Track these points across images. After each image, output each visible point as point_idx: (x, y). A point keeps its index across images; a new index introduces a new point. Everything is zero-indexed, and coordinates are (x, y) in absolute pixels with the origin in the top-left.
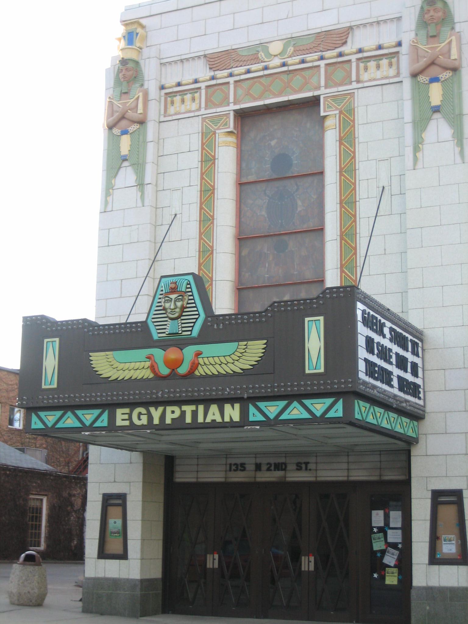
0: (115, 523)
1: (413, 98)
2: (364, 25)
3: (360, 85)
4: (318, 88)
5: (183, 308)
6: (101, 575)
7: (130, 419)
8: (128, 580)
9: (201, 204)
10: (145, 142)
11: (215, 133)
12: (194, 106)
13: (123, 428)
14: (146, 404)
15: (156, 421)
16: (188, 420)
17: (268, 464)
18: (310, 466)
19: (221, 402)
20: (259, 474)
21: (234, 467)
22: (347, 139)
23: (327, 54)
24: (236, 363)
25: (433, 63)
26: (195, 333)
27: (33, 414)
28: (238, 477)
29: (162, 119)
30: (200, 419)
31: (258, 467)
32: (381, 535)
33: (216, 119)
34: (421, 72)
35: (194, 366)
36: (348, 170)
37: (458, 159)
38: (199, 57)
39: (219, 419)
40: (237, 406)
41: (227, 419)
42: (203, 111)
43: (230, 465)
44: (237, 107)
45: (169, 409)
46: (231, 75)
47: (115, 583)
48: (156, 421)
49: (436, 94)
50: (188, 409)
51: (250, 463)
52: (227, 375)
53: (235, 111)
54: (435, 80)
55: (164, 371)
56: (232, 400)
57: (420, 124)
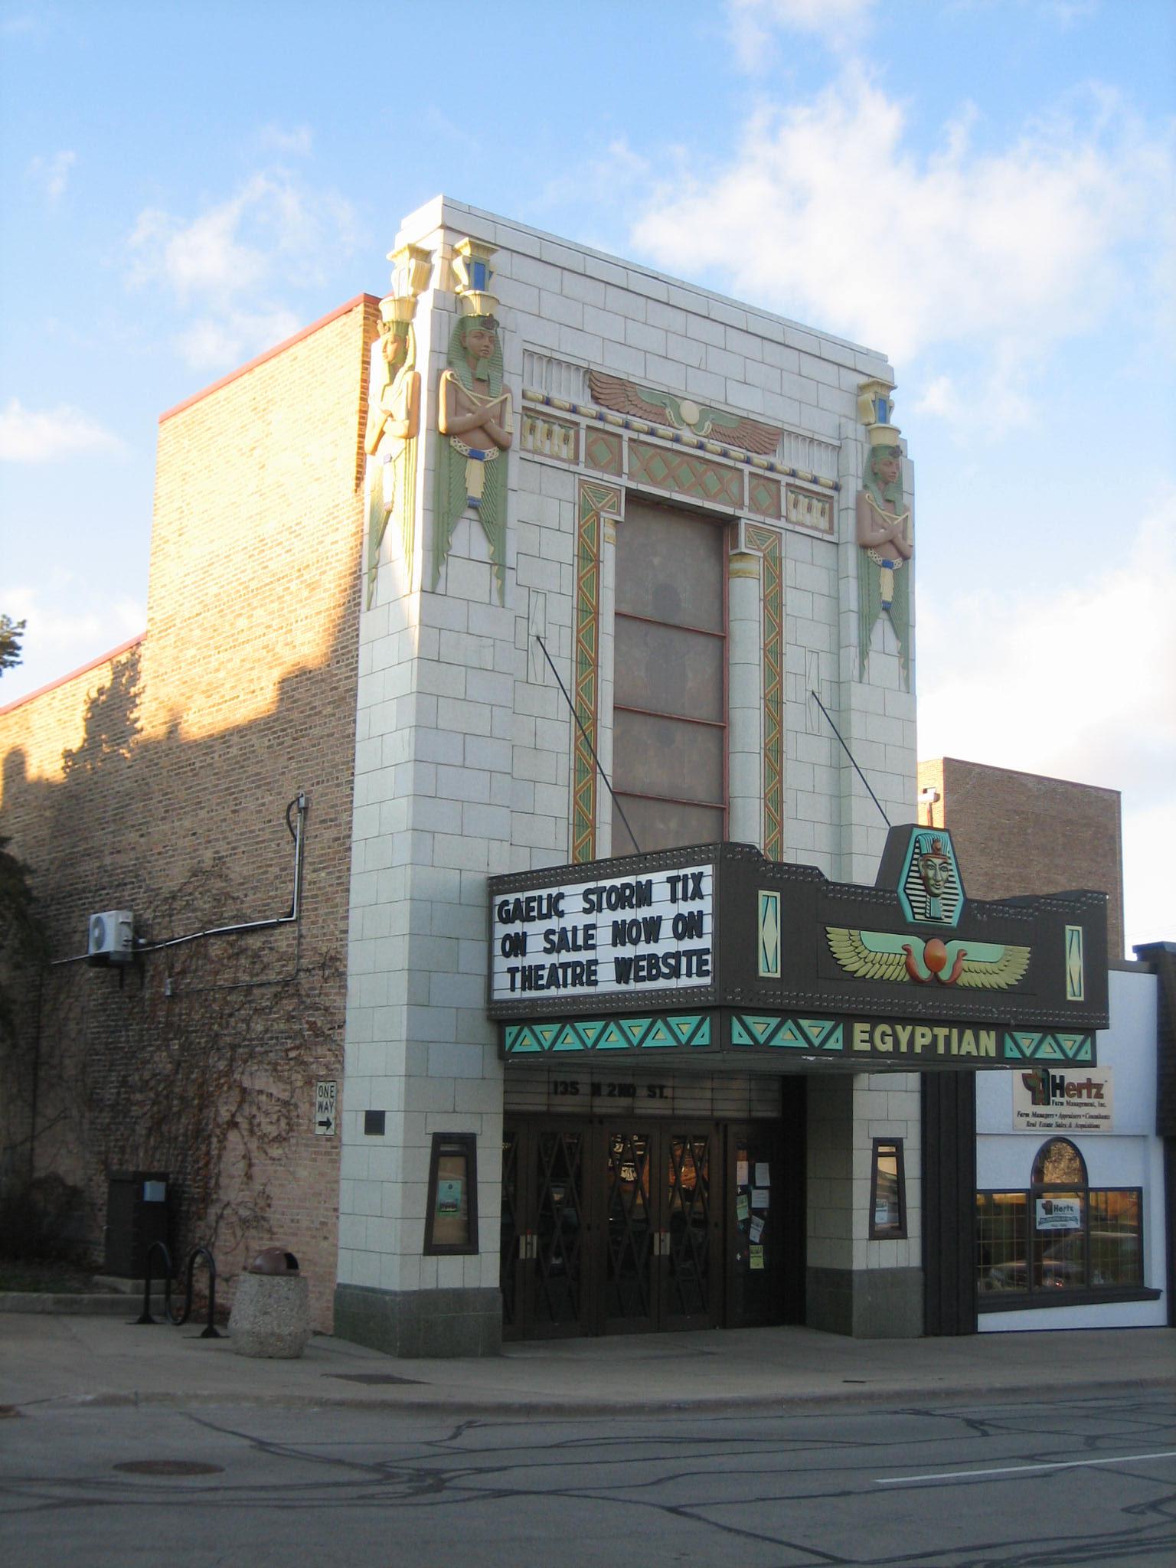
0: (450, 1187)
1: (859, 578)
3: (790, 527)
4: (741, 506)
6: (430, 1285)
7: (871, 1041)
8: (478, 1289)
11: (598, 515)
12: (566, 452)
13: (862, 1054)
14: (892, 1020)
15: (904, 1048)
16: (941, 1050)
17: (610, 1085)
18: (668, 1092)
19: (977, 1026)
20: (597, 1101)
21: (561, 1089)
22: (774, 605)
23: (756, 458)
26: (954, 922)
27: (734, 1019)
28: (568, 1104)
30: (954, 1051)
31: (596, 1090)
32: (744, 1197)
33: (602, 491)
37: (903, 688)
38: (578, 368)
40: (993, 1034)
41: (983, 1054)
43: (556, 1084)
44: (633, 485)
45: (919, 1030)
46: (627, 426)
47: (459, 1297)
48: (904, 1048)
50: (942, 1032)
51: (584, 1079)
53: (629, 491)
55: (924, 973)
56: (988, 1026)
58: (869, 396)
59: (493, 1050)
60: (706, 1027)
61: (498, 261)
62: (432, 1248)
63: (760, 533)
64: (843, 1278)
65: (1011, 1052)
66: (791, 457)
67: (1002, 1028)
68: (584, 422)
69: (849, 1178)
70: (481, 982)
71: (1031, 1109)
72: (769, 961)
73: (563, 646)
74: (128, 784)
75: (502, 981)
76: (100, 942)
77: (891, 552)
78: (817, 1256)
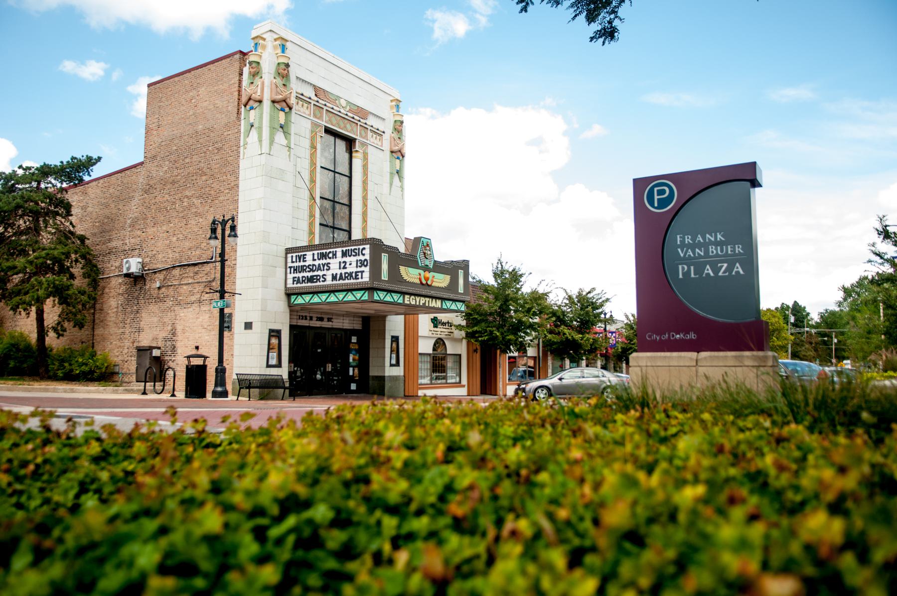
12: (307, 112)
22: (365, 167)
33: (318, 125)
35: (433, 281)
42: (312, 118)
50: (427, 299)
55: (424, 282)
58: (394, 103)
59: (286, 303)
60: (366, 294)
61: (288, 45)
62: (268, 366)
63: (364, 144)
64: (382, 379)
65: (445, 307)
66: (371, 121)
68: (313, 102)
69: (384, 348)
70: (283, 281)
71: (433, 329)
72: (385, 276)
73: (306, 176)
74: (136, 214)
75: (290, 281)
76: (128, 268)
77: (399, 154)
78: (373, 372)
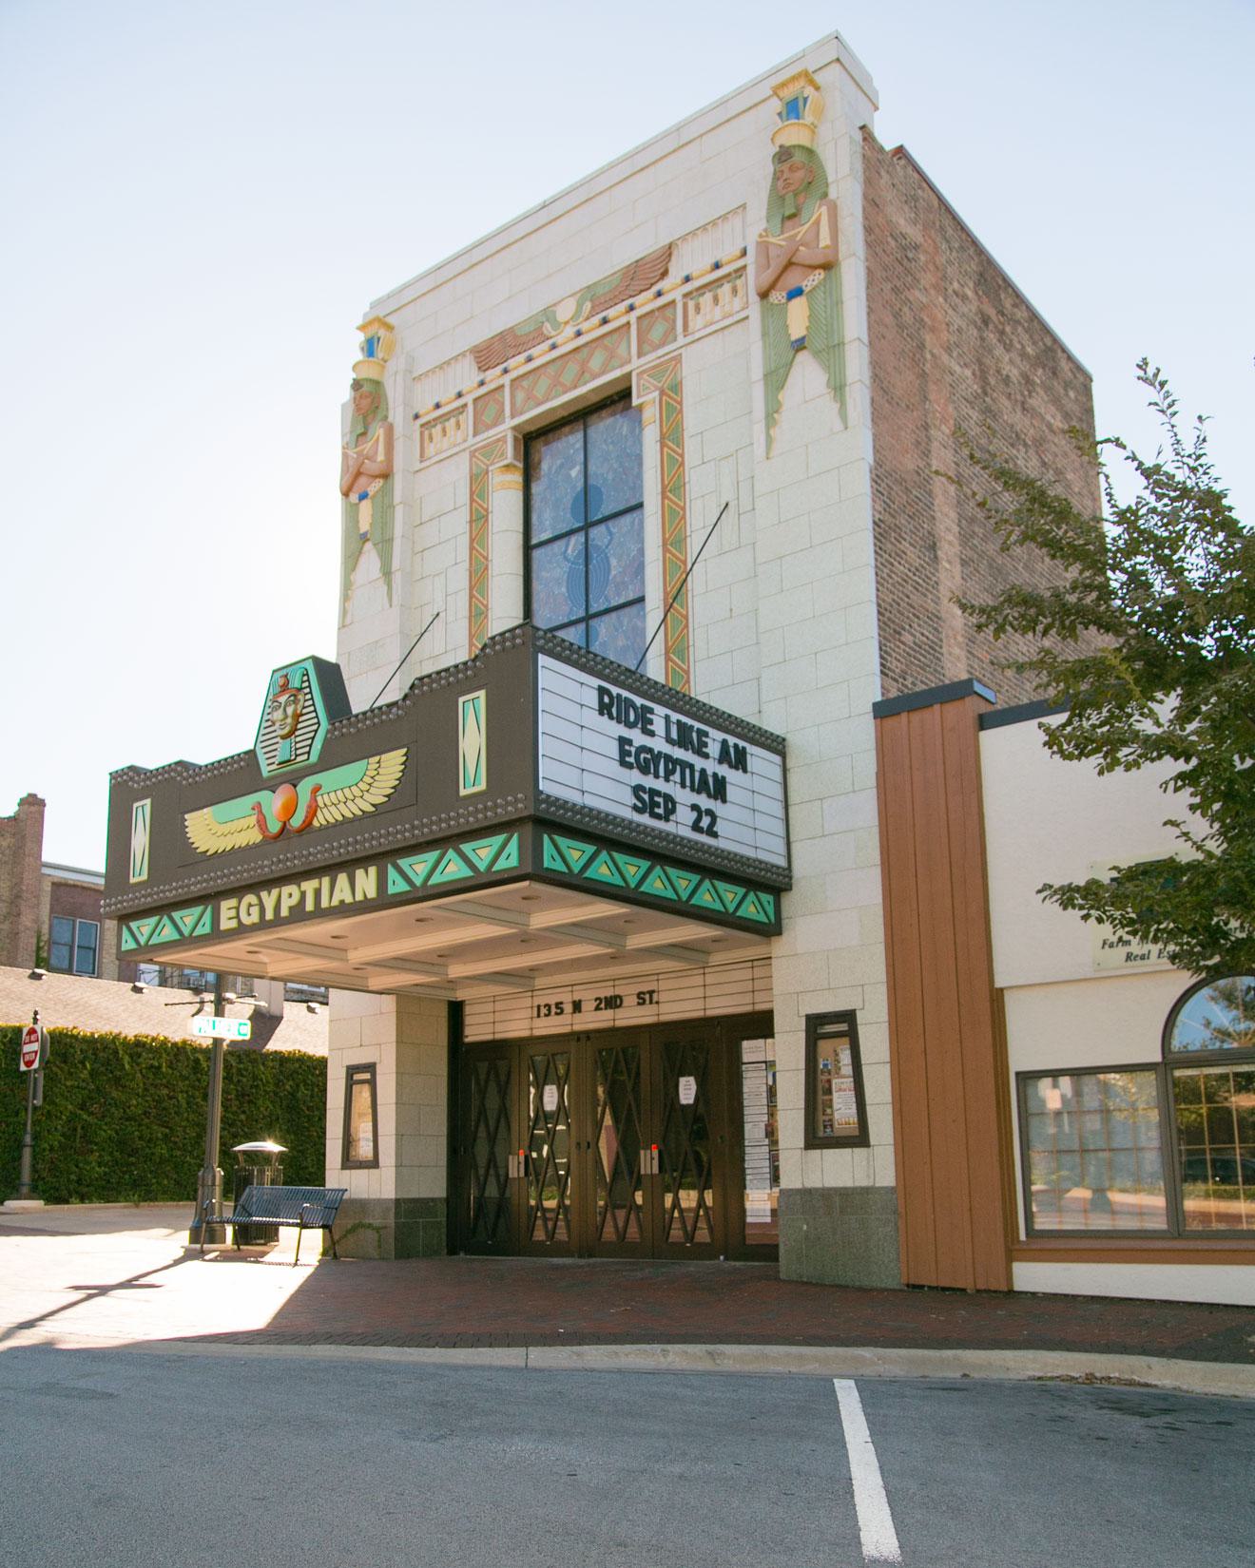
2: (693, 233)
3: (689, 339)
5: (297, 716)
9: (471, 589)
10: (392, 506)
19: (349, 865)
21: (544, 1011)
22: (672, 436)
24: (366, 796)
25: (790, 264)
29: (418, 466)
30: (325, 904)
31: (577, 1006)
33: (489, 450)
34: (772, 286)
35: (313, 811)
36: (673, 487)
39: (349, 899)
42: (471, 441)
49: (798, 317)
50: (309, 886)
52: (356, 819)
54: (796, 293)
56: (363, 861)
57: (776, 379)
67: (381, 858)
